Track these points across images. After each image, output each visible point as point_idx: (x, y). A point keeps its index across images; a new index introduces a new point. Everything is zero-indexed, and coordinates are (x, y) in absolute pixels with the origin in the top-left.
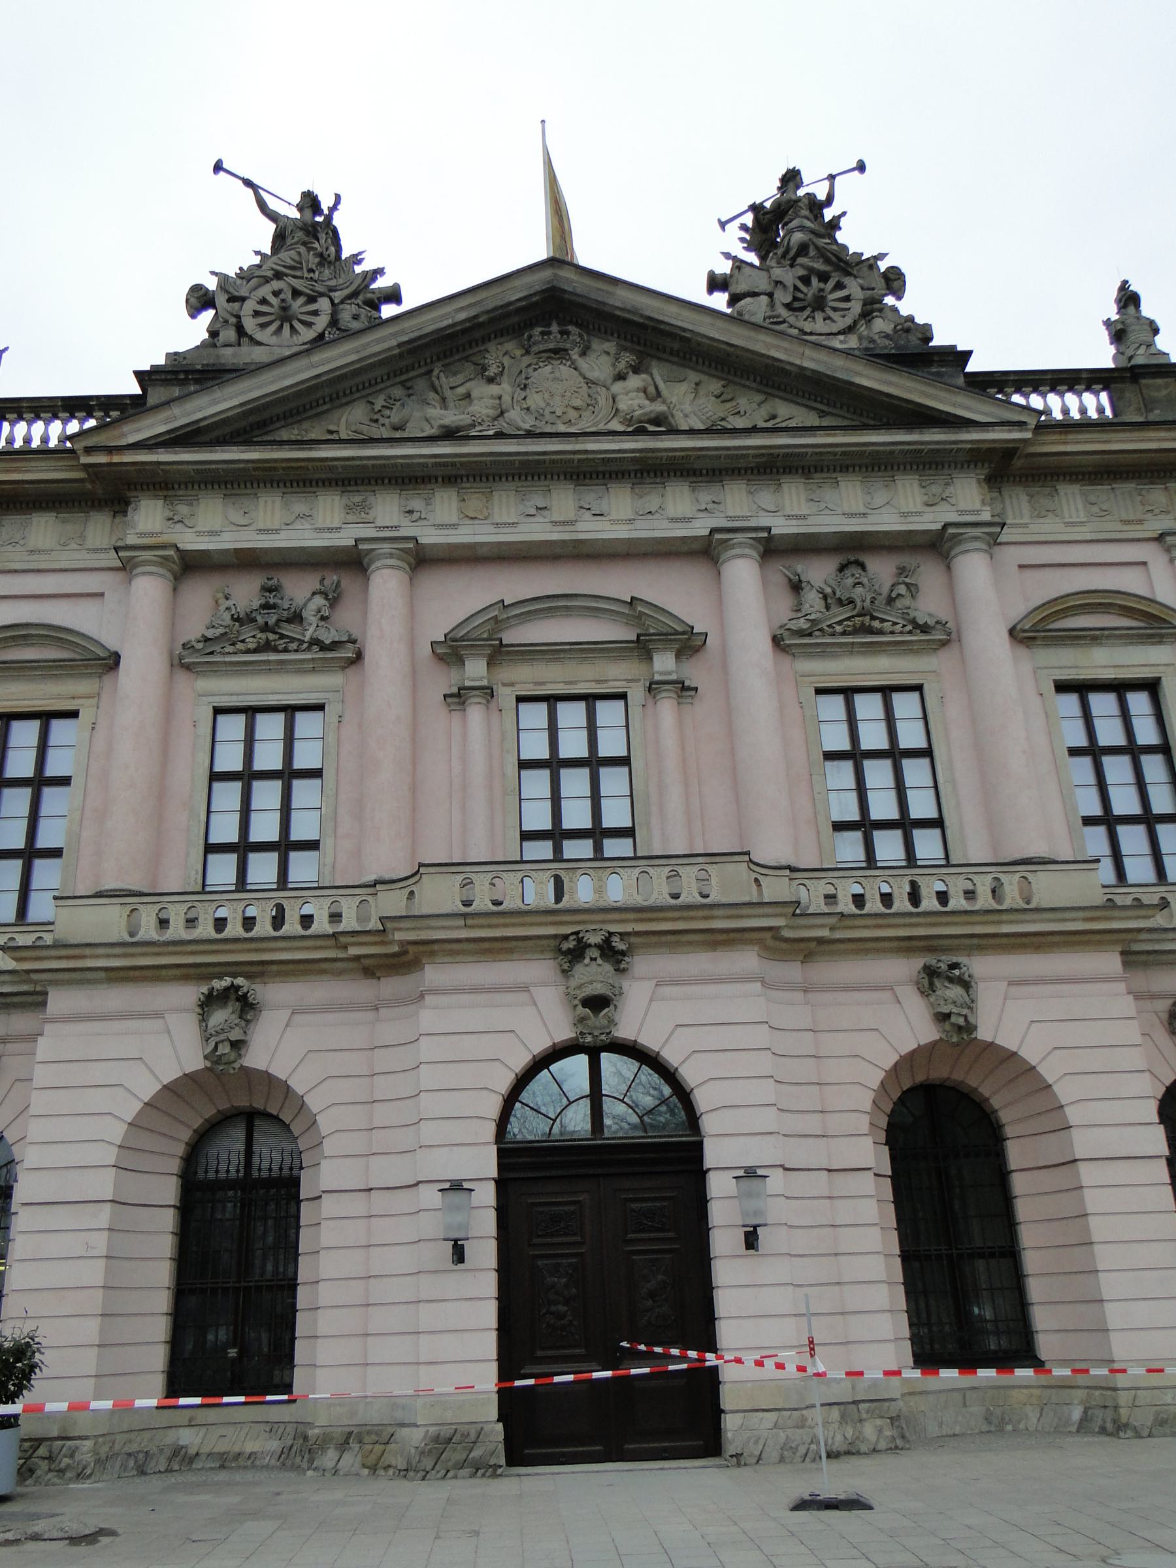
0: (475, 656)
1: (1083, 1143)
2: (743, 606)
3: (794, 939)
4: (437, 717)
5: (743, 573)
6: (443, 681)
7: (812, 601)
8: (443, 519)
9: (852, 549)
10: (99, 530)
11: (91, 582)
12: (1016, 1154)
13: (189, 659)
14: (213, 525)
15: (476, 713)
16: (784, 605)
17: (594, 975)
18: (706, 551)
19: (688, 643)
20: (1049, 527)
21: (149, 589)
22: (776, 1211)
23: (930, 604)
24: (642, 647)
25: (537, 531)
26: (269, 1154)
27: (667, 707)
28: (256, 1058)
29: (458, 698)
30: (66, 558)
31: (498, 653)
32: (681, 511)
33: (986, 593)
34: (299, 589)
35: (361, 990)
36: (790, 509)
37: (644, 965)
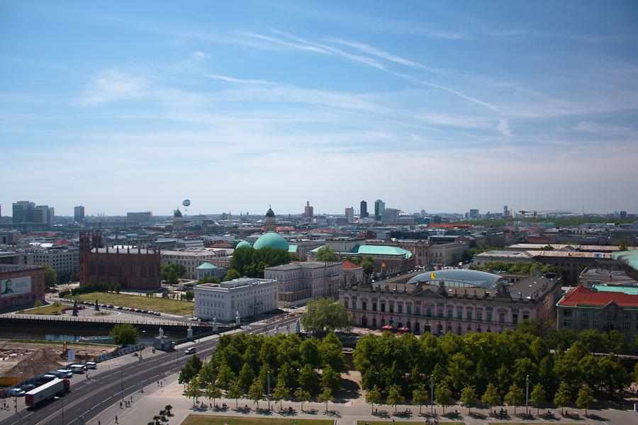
36: (437, 300)
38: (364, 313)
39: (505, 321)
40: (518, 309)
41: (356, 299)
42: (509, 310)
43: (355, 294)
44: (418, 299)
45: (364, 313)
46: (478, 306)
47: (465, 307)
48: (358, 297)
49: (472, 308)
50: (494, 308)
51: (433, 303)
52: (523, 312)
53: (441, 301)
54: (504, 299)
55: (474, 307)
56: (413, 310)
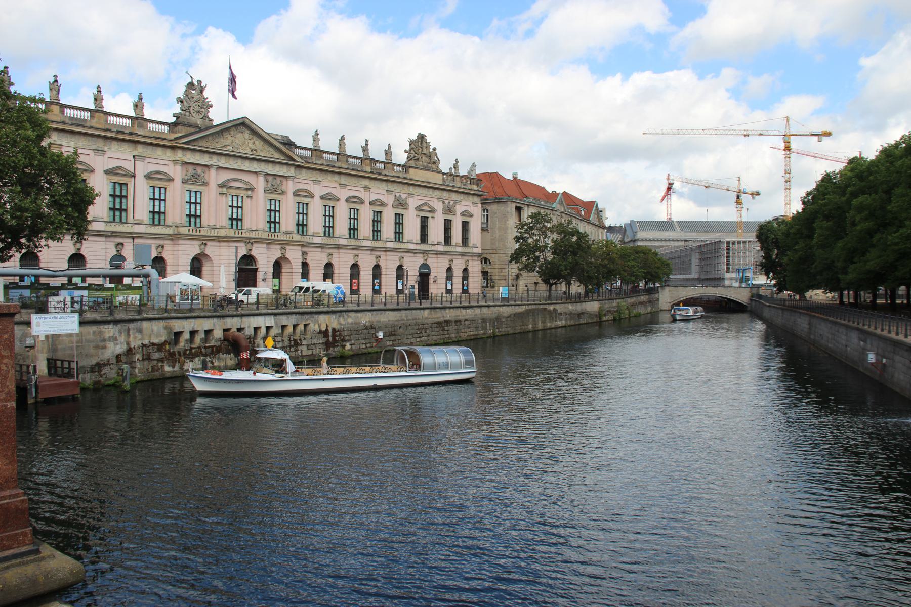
1: (294, 270)
2: (260, 183)
3: (269, 243)
5: (261, 179)
7: (269, 184)
8: (222, 162)
12: (283, 270)
13: (184, 181)
14: (190, 157)
17: (249, 246)
19: (253, 190)
20: (299, 176)
21: (179, 168)
23: (284, 188)
24: (247, 189)
27: (249, 199)
31: (229, 187)
32: (254, 167)
33: (290, 187)
34: (199, 170)
35: (217, 244)
36: (270, 169)
37: (255, 245)
42: (438, 206)
56: (176, 211)
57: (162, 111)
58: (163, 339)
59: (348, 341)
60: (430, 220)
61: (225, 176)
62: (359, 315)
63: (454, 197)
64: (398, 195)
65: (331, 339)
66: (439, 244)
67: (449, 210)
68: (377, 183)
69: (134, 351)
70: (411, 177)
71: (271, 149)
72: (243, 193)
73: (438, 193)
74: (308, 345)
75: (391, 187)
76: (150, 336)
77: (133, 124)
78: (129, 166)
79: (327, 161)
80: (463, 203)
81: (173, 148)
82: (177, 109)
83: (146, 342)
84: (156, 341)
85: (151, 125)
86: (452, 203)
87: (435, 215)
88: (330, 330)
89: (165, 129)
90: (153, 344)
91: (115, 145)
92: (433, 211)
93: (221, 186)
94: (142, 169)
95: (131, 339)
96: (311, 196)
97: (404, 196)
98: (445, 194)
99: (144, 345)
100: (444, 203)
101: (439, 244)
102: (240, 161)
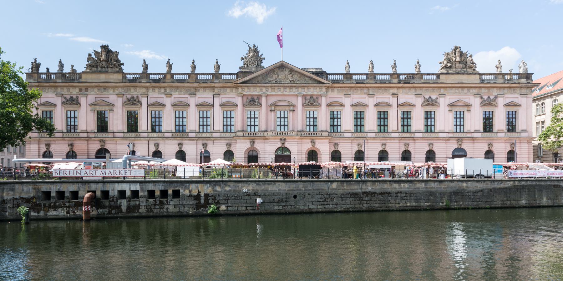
0: (273, 107)
2: (299, 102)
4: (269, 112)
5: (300, 99)
6: (269, 109)
9: (312, 96)
10: (234, 90)
11: (234, 96)
15: (273, 113)
16: (304, 101)
18: (297, 96)
19: (294, 106)
22: (296, 160)
24: (289, 106)
25: (279, 93)
26: (255, 154)
28: (255, 146)
29: (271, 111)
30: (232, 93)
36: (306, 92)
38: (102, 141)
39: (467, 128)
40: (496, 97)
41: (78, 104)
43: (74, 92)
44: (255, 91)
45: (102, 141)
46: (401, 101)
47: (371, 102)
48: (83, 100)
49: (389, 105)
50: (442, 101)
51: (293, 100)
52: (507, 105)
53: (314, 91)
54: (464, 78)
55: (393, 101)
57: (231, 66)
58: (32, 195)
59: (223, 204)
60: (466, 113)
61: (272, 100)
62: (240, 185)
63: (495, 92)
64: (427, 97)
65: (202, 202)
66: (476, 131)
67: (489, 103)
68: (404, 90)
69: (6, 201)
70: (442, 81)
71: (306, 78)
72: (287, 108)
73: (474, 91)
74: (175, 205)
75: (418, 91)
76: (21, 193)
77: (213, 77)
78: (210, 101)
79: (356, 80)
80: (506, 96)
81: (236, 87)
82: (241, 64)
83: (17, 197)
84: (24, 196)
85: (224, 77)
86: (492, 97)
87: (472, 109)
88: (202, 195)
89: (234, 77)
90: (23, 198)
91: (202, 90)
92: (468, 105)
93: (271, 105)
94: (217, 101)
95: (5, 194)
96: (342, 105)
97: (434, 97)
98: (483, 91)
99: (14, 199)
100: (481, 98)
101: (476, 131)
102: (282, 89)
